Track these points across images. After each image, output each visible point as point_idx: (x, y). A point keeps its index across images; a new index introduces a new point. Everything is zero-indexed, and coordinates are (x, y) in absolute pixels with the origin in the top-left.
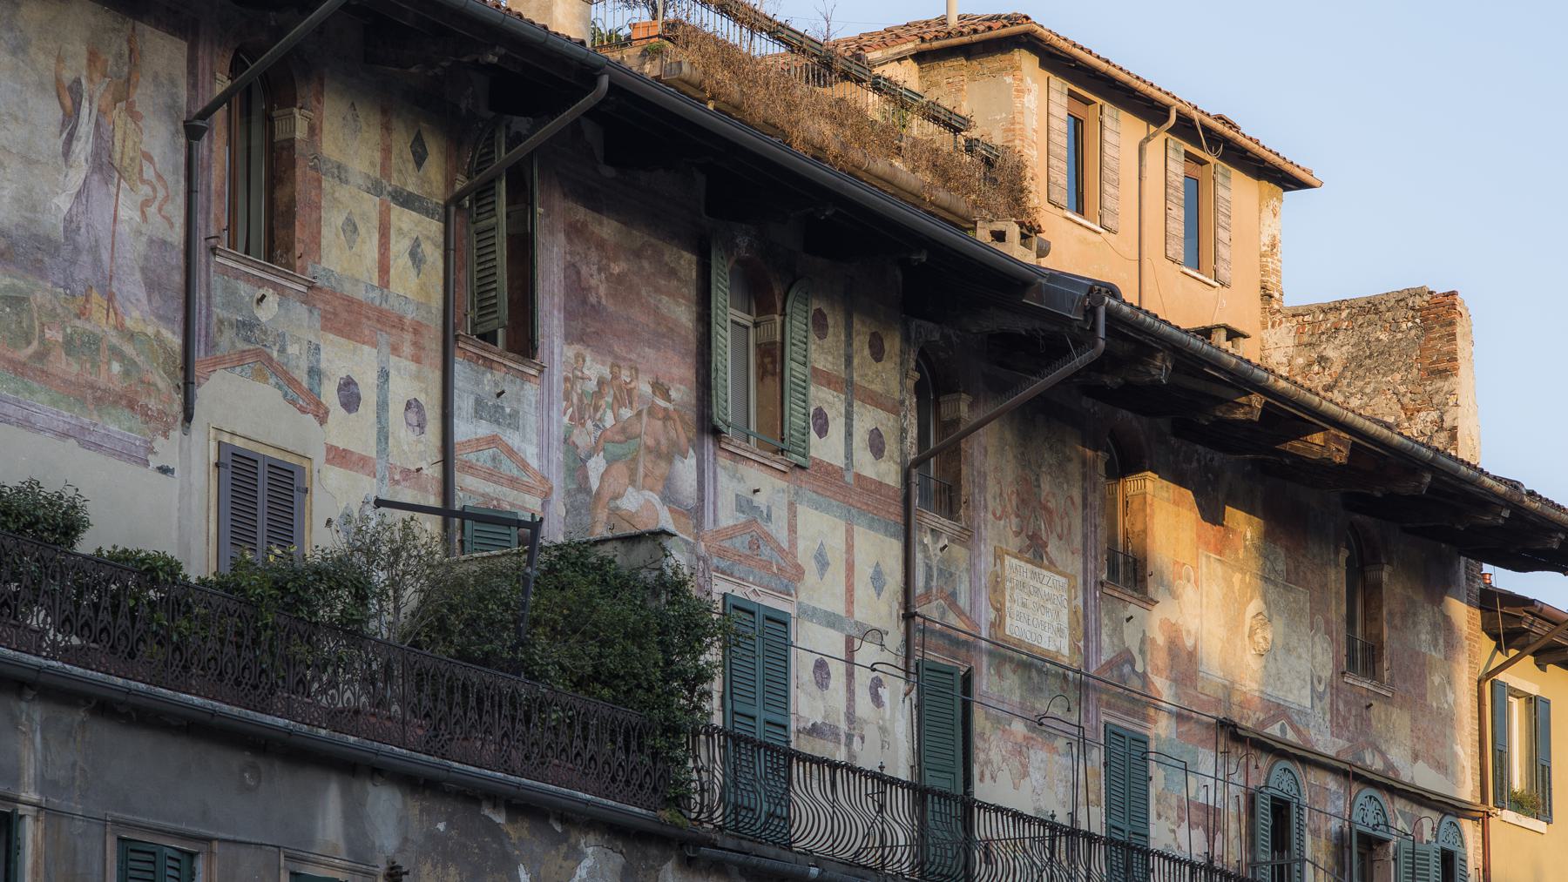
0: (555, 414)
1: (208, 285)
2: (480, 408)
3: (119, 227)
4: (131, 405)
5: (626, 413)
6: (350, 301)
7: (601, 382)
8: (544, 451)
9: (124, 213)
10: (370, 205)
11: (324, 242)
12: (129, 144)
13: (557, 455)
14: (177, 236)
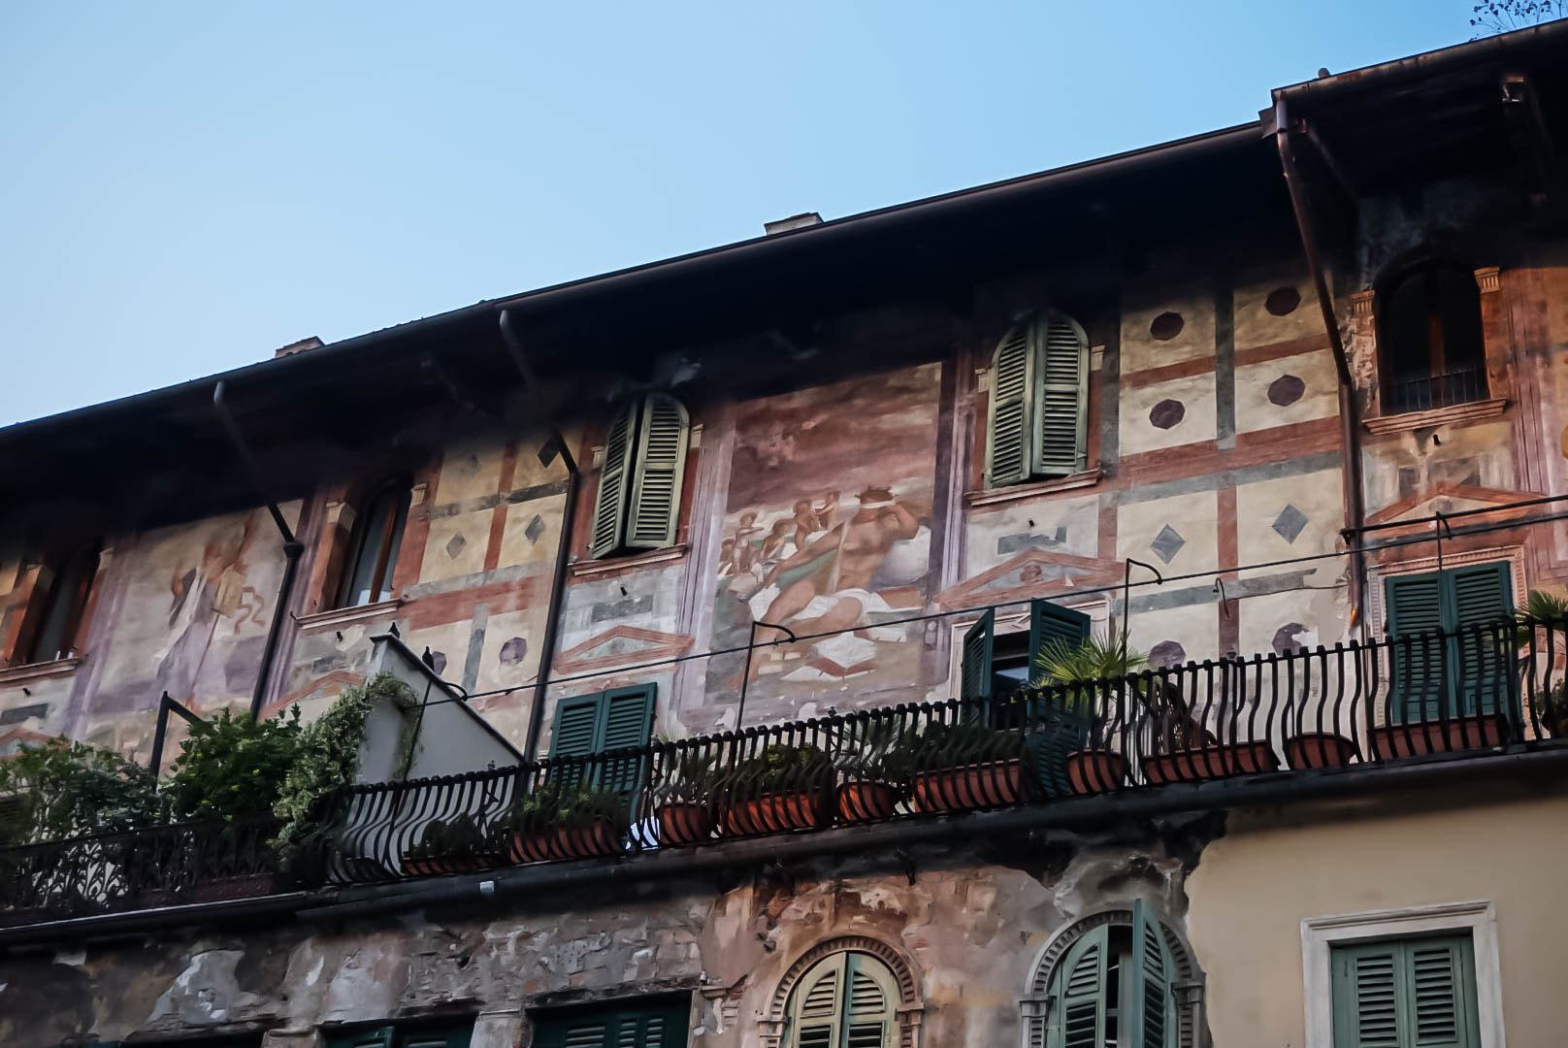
0: (705, 578)
7: (778, 528)
11: (423, 568)
12: (231, 589)
13: (705, 609)
14: (266, 630)
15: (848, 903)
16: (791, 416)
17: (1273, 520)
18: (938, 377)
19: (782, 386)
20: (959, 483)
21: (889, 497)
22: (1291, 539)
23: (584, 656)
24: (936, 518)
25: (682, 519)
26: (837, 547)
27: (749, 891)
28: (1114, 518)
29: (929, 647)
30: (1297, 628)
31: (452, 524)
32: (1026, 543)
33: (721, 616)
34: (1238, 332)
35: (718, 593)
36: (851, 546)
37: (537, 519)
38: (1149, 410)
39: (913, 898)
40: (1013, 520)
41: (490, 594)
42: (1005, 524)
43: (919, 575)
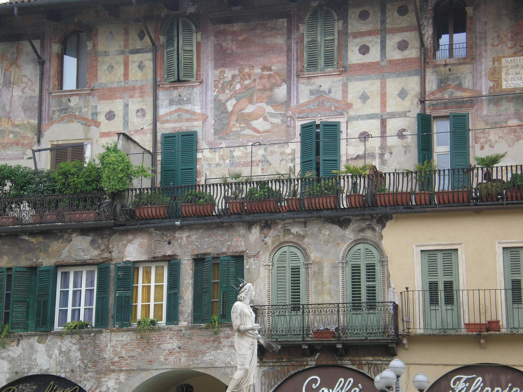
0: (209, 93)
1: (49, 103)
2: (171, 102)
3: (13, 98)
4: (17, 144)
5: (247, 82)
6: (110, 89)
7: (234, 77)
8: (204, 105)
9: (15, 94)
10: (120, 58)
11: (99, 76)
12: (17, 75)
13: (211, 105)
14: (37, 93)
15: (287, 232)
16: (233, 33)
17: (398, 92)
18: (286, 25)
19: (228, 21)
20: (295, 67)
21: (271, 71)
22: (403, 99)
23: (168, 118)
24: (288, 80)
25: (198, 70)
26: (255, 87)
27: (258, 227)
28: (347, 87)
29: (289, 127)
30: (404, 130)
31: (107, 59)
32: (318, 93)
33: (216, 109)
34: (388, 21)
35: (215, 100)
36: (259, 87)
37: (141, 62)
38: (358, 47)
39: (306, 231)
40: (314, 84)
41: (128, 90)
42: (311, 85)
43: (284, 100)
